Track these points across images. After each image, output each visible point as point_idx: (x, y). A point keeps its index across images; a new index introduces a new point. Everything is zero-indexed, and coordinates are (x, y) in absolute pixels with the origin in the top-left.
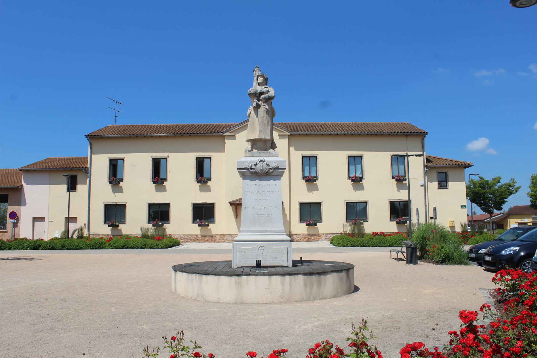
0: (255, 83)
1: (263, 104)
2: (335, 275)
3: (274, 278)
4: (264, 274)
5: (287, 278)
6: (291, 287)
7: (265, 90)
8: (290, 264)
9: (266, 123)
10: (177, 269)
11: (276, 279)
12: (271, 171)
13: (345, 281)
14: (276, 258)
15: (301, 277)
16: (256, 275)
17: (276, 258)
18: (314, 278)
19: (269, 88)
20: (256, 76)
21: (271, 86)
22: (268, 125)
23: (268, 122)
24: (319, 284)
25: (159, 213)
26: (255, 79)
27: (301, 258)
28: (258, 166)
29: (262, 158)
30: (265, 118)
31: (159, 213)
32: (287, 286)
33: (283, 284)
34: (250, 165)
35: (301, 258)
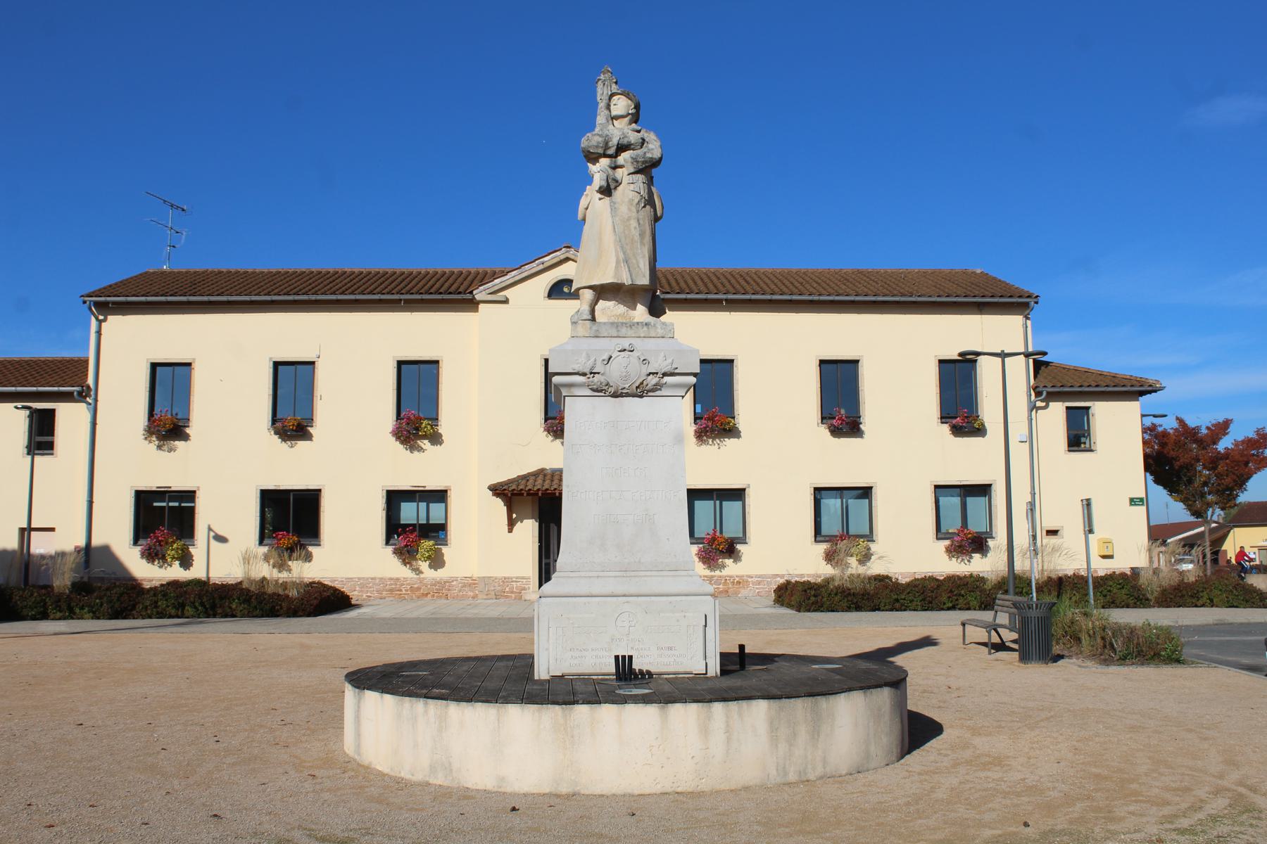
0: (601, 119)
1: (626, 179)
2: (857, 698)
3: (677, 710)
4: (646, 700)
5: (718, 707)
6: (729, 740)
7: (633, 138)
8: (714, 668)
9: (637, 238)
10: (365, 679)
11: (685, 715)
12: (653, 380)
13: (887, 718)
15: (761, 707)
16: (624, 700)
18: (799, 706)
19: (644, 134)
20: (605, 98)
21: (649, 129)
22: (642, 243)
23: (642, 235)
24: (815, 733)
25: (291, 517)
26: (602, 105)
27: (742, 647)
28: (613, 363)
29: (625, 343)
30: (634, 223)
31: (291, 517)
32: (718, 738)
33: (705, 731)
34: (590, 364)
35: (742, 647)
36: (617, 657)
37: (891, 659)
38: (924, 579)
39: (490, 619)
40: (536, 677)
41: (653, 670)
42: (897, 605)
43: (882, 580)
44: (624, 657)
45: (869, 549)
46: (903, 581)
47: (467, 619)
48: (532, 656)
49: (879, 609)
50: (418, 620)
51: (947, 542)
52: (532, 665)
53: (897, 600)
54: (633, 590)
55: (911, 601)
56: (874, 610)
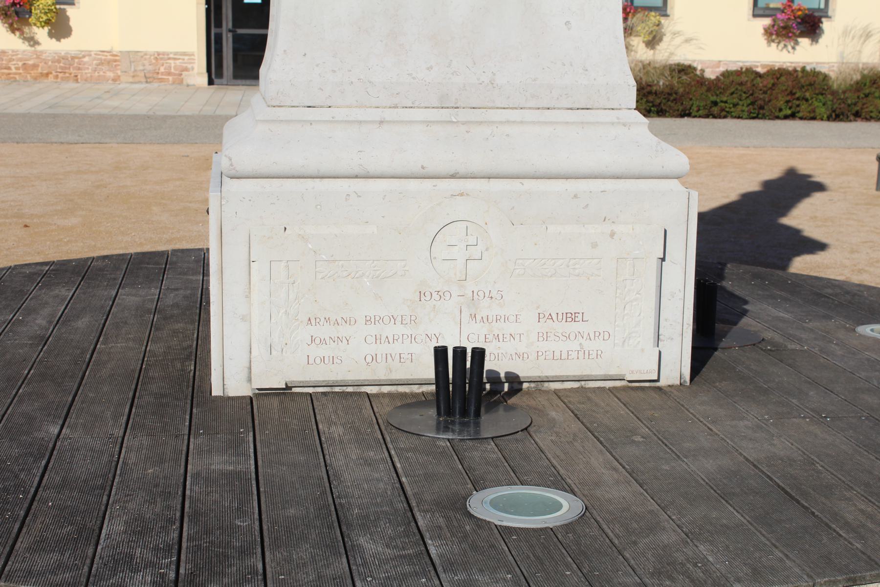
14: (572, 317)
17: (572, 317)
36: (440, 353)
37: (786, 221)
38: (739, 73)
39: (135, 117)
40: (216, 391)
41: (523, 371)
42: (715, 110)
43: (684, 70)
44: (460, 352)
45: (659, 25)
46: (711, 74)
47: (101, 117)
48: (199, 261)
49: (689, 115)
50: (27, 117)
51: (767, 21)
52: (199, 307)
53: (715, 103)
54: (477, 164)
55: (735, 105)
56: (682, 116)
